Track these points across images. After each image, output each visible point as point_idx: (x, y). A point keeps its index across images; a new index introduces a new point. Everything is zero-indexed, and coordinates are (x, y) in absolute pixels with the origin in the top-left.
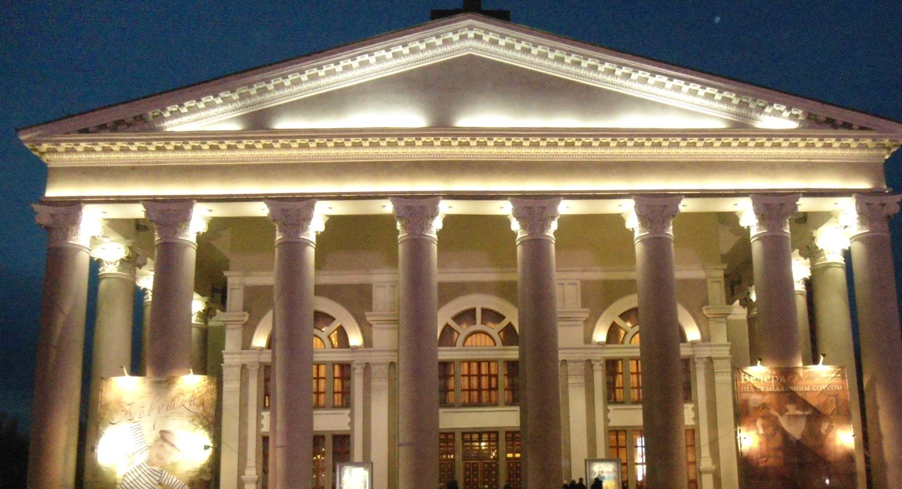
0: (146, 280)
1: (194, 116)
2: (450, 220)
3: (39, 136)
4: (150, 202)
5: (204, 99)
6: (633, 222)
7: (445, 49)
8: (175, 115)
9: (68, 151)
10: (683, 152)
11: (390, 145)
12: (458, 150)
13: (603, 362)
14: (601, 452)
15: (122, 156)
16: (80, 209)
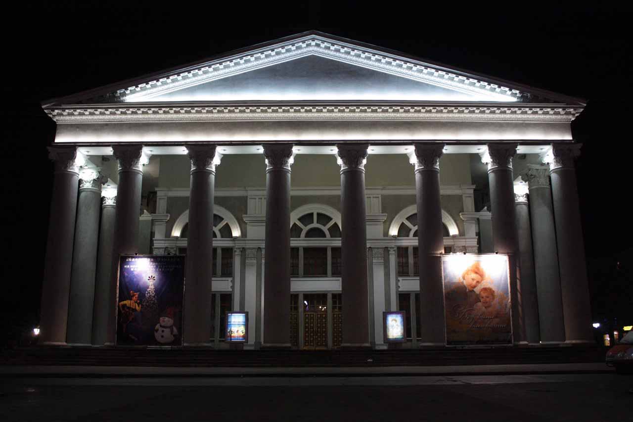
0: (110, 193)
1: (144, 93)
2: (298, 157)
3: (54, 105)
4: (116, 146)
5: (150, 83)
6: (414, 160)
7: (297, 52)
8: (132, 92)
9: (69, 114)
10: (445, 116)
11: (262, 111)
12: (305, 115)
13: (395, 249)
14: (394, 307)
15: (101, 117)
16: (75, 150)
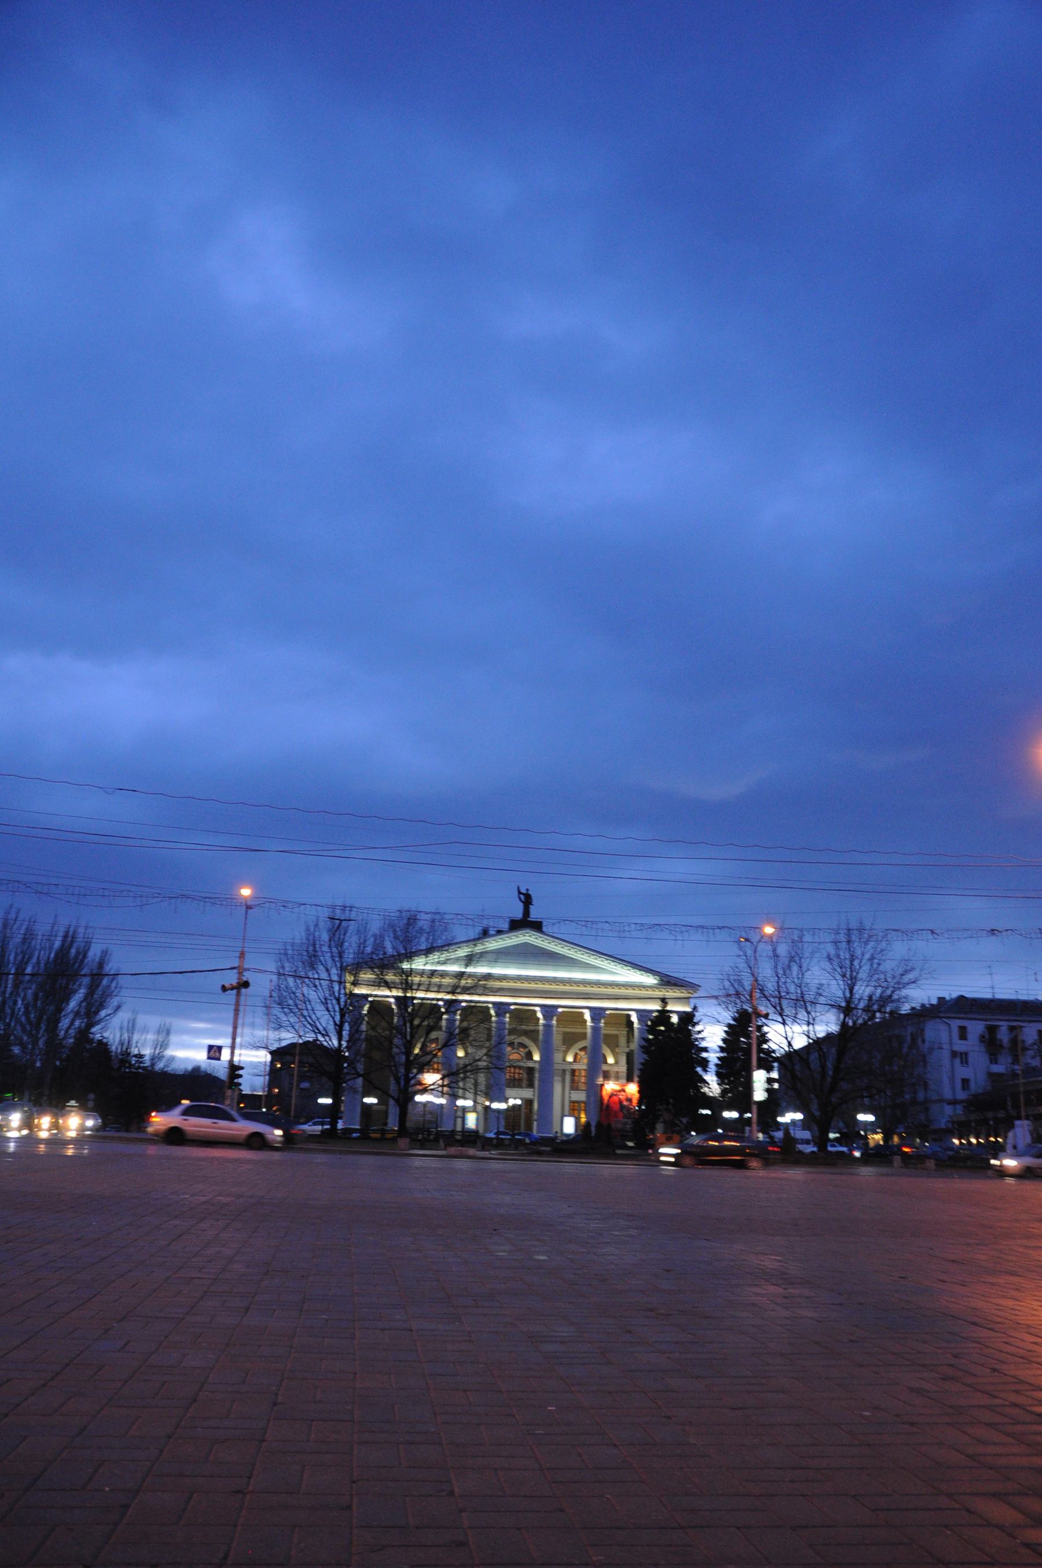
6: (587, 1016)
14: (567, 1112)
